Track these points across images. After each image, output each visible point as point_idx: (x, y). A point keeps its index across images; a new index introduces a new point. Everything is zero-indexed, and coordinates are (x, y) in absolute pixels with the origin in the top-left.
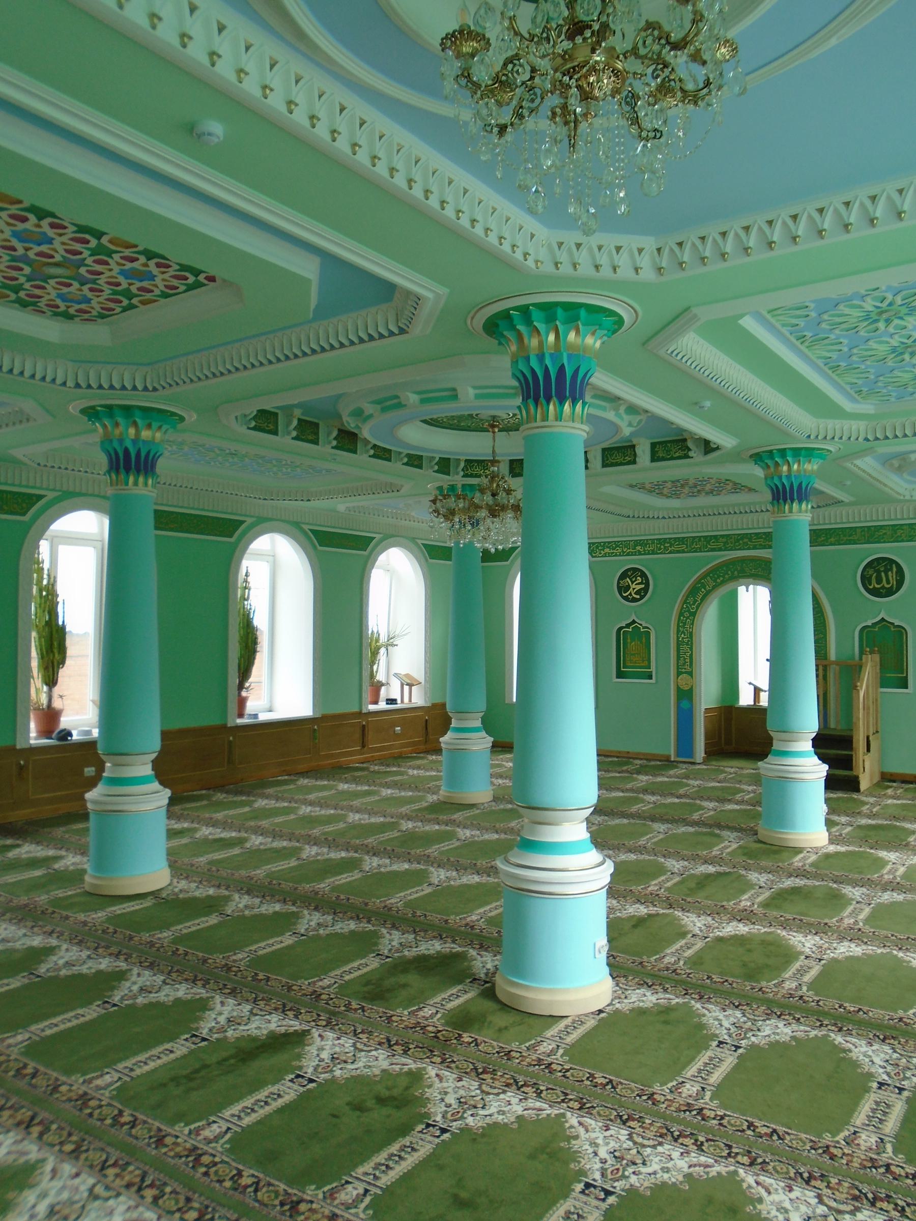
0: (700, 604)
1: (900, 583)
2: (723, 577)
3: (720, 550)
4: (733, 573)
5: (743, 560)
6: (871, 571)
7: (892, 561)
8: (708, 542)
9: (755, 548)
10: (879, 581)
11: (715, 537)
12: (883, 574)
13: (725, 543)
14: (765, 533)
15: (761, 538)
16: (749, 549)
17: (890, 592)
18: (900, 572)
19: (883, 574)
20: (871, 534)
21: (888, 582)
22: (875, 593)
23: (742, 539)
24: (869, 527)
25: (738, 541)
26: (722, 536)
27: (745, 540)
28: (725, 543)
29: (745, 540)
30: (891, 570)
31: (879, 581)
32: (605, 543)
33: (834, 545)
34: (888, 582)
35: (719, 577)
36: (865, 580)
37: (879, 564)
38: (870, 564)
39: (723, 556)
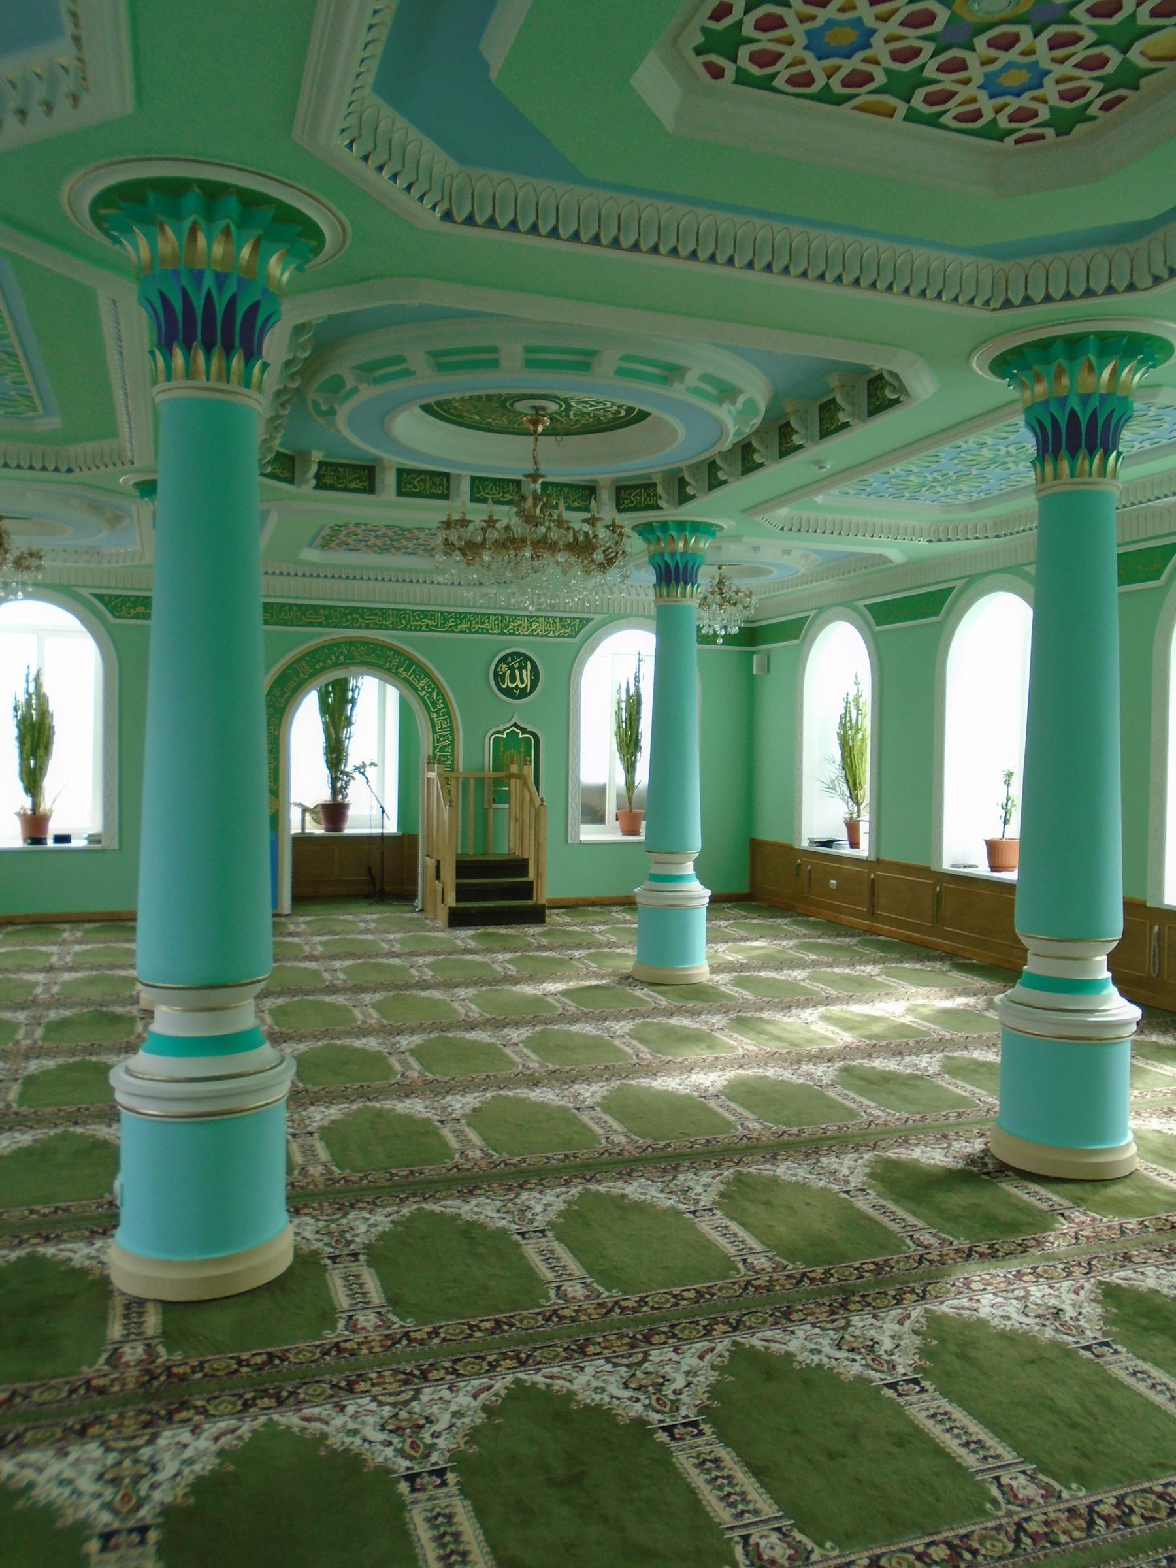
0: (290, 697)
1: (534, 683)
2: (324, 661)
3: (320, 625)
4: (337, 658)
5: (351, 642)
6: (505, 667)
7: (526, 658)
8: (304, 613)
9: (367, 627)
10: (513, 680)
11: (314, 607)
12: (517, 672)
13: (327, 617)
14: (381, 610)
15: (376, 614)
16: (360, 627)
17: (524, 694)
18: (535, 670)
19: (517, 672)
20: (505, 623)
21: (522, 682)
22: (508, 692)
23: (351, 613)
24: (503, 616)
25: (345, 615)
26: (324, 607)
27: (355, 616)
28: (327, 617)
29: (355, 616)
30: (525, 667)
31: (513, 680)
32: (137, 597)
33: (465, 632)
34: (522, 682)
35: (318, 662)
36: (499, 678)
37: (513, 660)
38: (503, 660)
39: (321, 634)
